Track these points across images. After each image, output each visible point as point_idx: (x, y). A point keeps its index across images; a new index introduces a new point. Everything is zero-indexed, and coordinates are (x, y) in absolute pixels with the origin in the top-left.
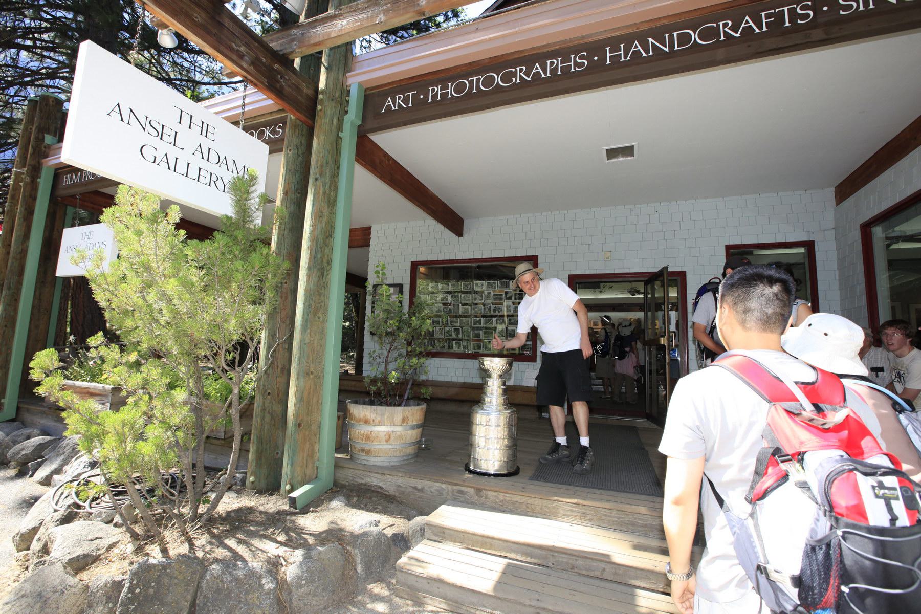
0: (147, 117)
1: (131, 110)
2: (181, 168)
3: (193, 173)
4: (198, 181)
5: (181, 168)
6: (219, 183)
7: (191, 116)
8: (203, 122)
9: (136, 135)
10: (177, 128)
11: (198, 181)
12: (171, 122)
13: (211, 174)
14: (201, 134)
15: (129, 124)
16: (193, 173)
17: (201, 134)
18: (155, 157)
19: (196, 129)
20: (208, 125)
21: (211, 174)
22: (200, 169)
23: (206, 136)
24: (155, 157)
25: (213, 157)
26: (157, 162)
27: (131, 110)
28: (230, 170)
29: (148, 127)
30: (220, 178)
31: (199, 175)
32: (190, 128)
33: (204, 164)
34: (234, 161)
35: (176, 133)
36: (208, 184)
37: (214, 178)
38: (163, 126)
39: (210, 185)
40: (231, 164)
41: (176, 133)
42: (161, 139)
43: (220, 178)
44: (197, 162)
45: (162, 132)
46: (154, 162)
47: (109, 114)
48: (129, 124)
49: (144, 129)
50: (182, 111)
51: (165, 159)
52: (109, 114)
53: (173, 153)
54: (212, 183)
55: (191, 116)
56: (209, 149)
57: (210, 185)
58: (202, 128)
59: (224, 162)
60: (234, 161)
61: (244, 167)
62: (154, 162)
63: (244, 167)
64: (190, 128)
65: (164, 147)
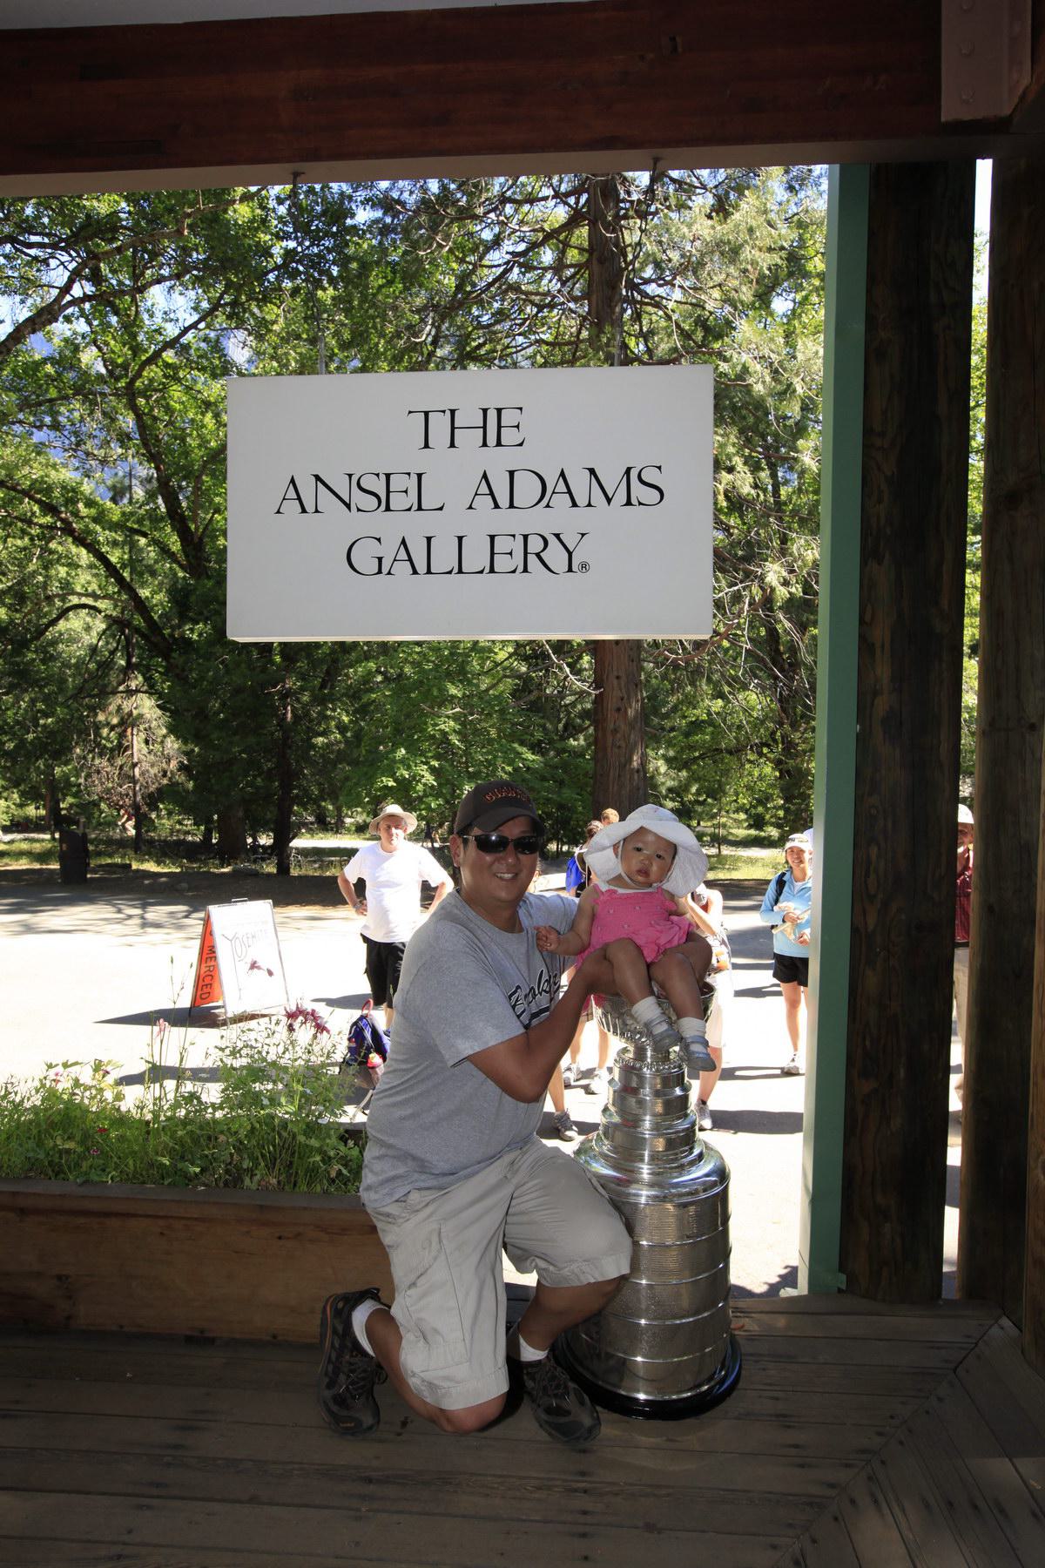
0: (350, 476)
1: (318, 478)
2: (444, 557)
3: (476, 557)
5: (444, 557)
6: (555, 555)
8: (485, 411)
9: (337, 525)
10: (421, 461)
11: (492, 571)
12: (402, 453)
13: (526, 537)
14: (485, 444)
15: (317, 511)
16: (476, 557)
17: (485, 444)
18: (380, 559)
19: (468, 439)
20: (499, 411)
21: (526, 537)
22: (492, 538)
23: (499, 444)
24: (380, 559)
25: (527, 489)
26: (385, 569)
28: (582, 500)
29: (359, 499)
31: (492, 554)
32: (452, 445)
33: (506, 521)
34: (592, 471)
35: (420, 476)
36: (521, 568)
37: (535, 545)
38: (388, 476)
39: (525, 570)
40: (580, 484)
41: (420, 476)
42: (388, 509)
43: (552, 541)
44: (486, 519)
46: (380, 572)
47: (278, 512)
48: (317, 511)
49: (348, 506)
50: (426, 414)
51: (403, 555)
53: (415, 527)
54: (532, 559)
55: (453, 412)
56: (512, 473)
57: (525, 570)
58: (484, 427)
59: (561, 487)
60: (592, 471)
61: (628, 471)
62: (380, 572)
63: (628, 471)
64: (452, 445)
65: (392, 527)
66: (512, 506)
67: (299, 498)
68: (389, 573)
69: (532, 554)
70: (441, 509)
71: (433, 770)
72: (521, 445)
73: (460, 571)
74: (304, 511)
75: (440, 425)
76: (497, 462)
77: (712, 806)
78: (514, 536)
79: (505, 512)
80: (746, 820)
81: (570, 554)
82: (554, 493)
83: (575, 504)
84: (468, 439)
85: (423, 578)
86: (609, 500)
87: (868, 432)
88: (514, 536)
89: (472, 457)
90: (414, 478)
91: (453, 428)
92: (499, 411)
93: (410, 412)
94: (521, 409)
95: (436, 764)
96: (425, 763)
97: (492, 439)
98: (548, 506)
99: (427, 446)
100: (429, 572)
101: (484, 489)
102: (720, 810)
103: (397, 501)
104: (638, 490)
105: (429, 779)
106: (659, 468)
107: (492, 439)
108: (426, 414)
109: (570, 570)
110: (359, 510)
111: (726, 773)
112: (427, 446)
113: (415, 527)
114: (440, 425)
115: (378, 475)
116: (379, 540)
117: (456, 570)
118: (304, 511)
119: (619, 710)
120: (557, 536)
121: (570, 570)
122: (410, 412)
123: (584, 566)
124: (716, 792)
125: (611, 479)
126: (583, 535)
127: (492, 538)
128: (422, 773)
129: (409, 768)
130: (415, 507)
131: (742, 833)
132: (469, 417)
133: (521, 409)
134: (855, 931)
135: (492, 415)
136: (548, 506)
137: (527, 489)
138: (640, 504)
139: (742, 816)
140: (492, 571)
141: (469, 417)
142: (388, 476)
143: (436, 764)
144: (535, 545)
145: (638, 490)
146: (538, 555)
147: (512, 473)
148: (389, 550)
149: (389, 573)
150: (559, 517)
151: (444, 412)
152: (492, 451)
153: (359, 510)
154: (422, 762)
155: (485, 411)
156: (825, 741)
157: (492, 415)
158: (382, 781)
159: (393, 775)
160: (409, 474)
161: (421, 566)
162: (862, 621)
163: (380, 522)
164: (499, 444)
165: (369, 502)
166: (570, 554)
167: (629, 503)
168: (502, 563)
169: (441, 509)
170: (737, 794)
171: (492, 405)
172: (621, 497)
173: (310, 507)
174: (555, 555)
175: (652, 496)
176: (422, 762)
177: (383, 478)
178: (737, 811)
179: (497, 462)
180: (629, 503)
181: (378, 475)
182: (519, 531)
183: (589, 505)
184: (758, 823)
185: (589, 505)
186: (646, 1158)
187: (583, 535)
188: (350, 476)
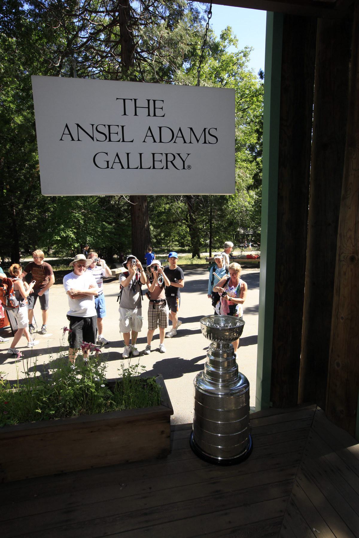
0: (93, 125)
1: (78, 125)
2: (134, 162)
4: (154, 168)
5: (134, 162)
6: (178, 162)
7: (135, 100)
8: (149, 101)
10: (123, 120)
13: (167, 154)
14: (149, 115)
15: (79, 140)
16: (147, 162)
17: (149, 115)
18: (108, 162)
19: (142, 112)
20: (154, 101)
21: (167, 154)
22: (153, 154)
23: (155, 115)
24: (108, 162)
26: (110, 166)
27: (78, 125)
28: (188, 141)
29: (97, 135)
30: (177, 156)
32: (136, 115)
33: (158, 148)
34: (191, 129)
35: (123, 127)
36: (165, 167)
37: (170, 158)
38: (109, 126)
39: (167, 168)
40: (187, 133)
41: (123, 127)
42: (110, 140)
43: (177, 156)
44: (150, 147)
45: (110, 133)
48: (79, 140)
49: (93, 138)
50: (124, 100)
52: (61, 140)
53: (122, 149)
54: (169, 163)
55: (135, 100)
56: (160, 128)
57: (167, 168)
58: (149, 108)
59: (180, 135)
60: (191, 129)
61: (205, 129)
62: (108, 167)
63: (205, 129)
64: (136, 115)
65: (113, 148)
66: (161, 141)
67: (70, 134)
68: (112, 168)
70: (132, 141)
71: (74, 233)
72: (163, 116)
73: (141, 168)
74: (73, 140)
75: (130, 105)
76: (155, 123)
77: (167, 240)
78: (162, 154)
79: (158, 144)
80: (178, 244)
81: (184, 162)
82: (177, 137)
83: (185, 142)
84: (142, 112)
85: (126, 170)
86: (198, 141)
87: (281, 119)
88: (162, 154)
90: (121, 128)
91: (136, 107)
92: (154, 101)
93: (117, 99)
94: (163, 101)
95: (75, 230)
96: (71, 231)
97: (152, 113)
98: (175, 142)
99: (125, 114)
100: (128, 168)
101: (149, 134)
102: (170, 241)
103: (114, 137)
104: (208, 137)
105: (73, 236)
106: (216, 129)
107: (152, 113)
108: (124, 100)
109: (184, 168)
110: (97, 140)
111: (171, 229)
112: (125, 114)
113: (122, 149)
114: (130, 105)
115: (105, 125)
116: (107, 154)
117: (139, 167)
118: (73, 140)
119: (139, 209)
120: (179, 154)
121: (184, 168)
122: (117, 99)
123: (189, 167)
124: (168, 235)
125: (199, 132)
126: (188, 154)
127: (153, 154)
128: (71, 234)
129: (65, 233)
130: (121, 140)
131: (177, 248)
132: (143, 103)
133: (163, 101)
134: (276, 294)
135: (151, 103)
136: (175, 142)
137: (167, 135)
138: (209, 143)
139: (177, 243)
140: (154, 168)
142: (109, 126)
143: (75, 230)
144: (170, 158)
145: (208, 137)
146: (172, 162)
147: (160, 128)
148: (111, 158)
149: (112, 168)
150: (179, 147)
151: (132, 100)
152: (152, 118)
153: (97, 140)
154: (70, 230)
155: (149, 101)
156: (267, 231)
157: (151, 103)
158: (55, 238)
159: (59, 235)
160: (118, 126)
161: (125, 166)
162: (279, 189)
163: (106, 146)
164: (155, 115)
165: (102, 137)
166: (184, 162)
167: (205, 142)
168: (157, 165)
169: (132, 141)
170: (174, 236)
171: (152, 98)
172: (202, 140)
173: (76, 138)
174: (178, 162)
175: (213, 140)
176: (70, 230)
177: (107, 127)
178: (176, 241)
179: (155, 123)
180: (205, 142)
181: (105, 125)
182: (164, 152)
183: (190, 143)
184: (182, 245)
185: (190, 143)
186: (221, 381)
187: (188, 154)
188: (93, 125)
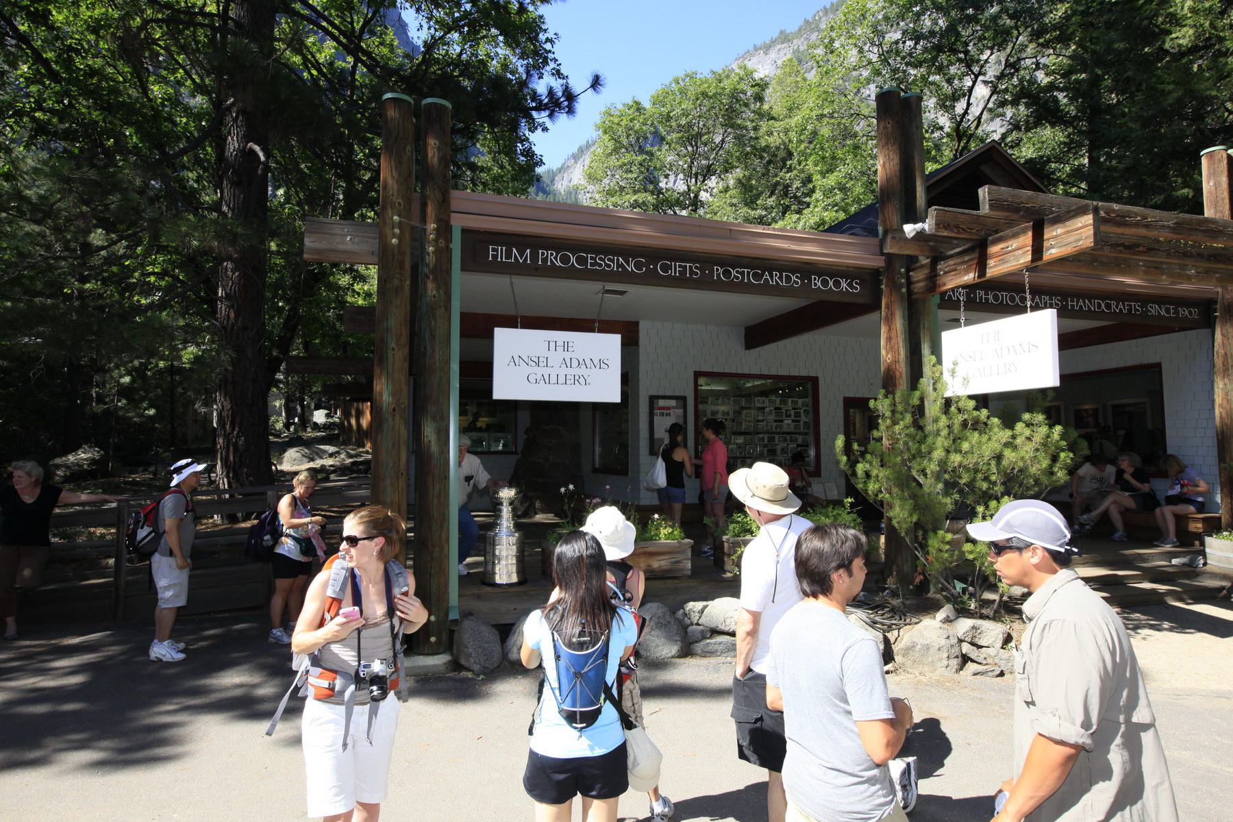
2: (554, 380)
3: (562, 380)
5: (554, 380)
6: (582, 380)
9: (524, 370)
12: (543, 352)
16: (562, 380)
19: (560, 349)
25: (575, 363)
29: (531, 363)
33: (569, 371)
37: (577, 378)
44: (564, 371)
53: (546, 371)
65: (541, 371)
69: (576, 380)
76: (567, 356)
89: (561, 354)
132: (560, 343)
137: (575, 363)
141: (560, 343)
148: (539, 377)
150: (582, 371)
174: (582, 380)
179: (567, 356)
